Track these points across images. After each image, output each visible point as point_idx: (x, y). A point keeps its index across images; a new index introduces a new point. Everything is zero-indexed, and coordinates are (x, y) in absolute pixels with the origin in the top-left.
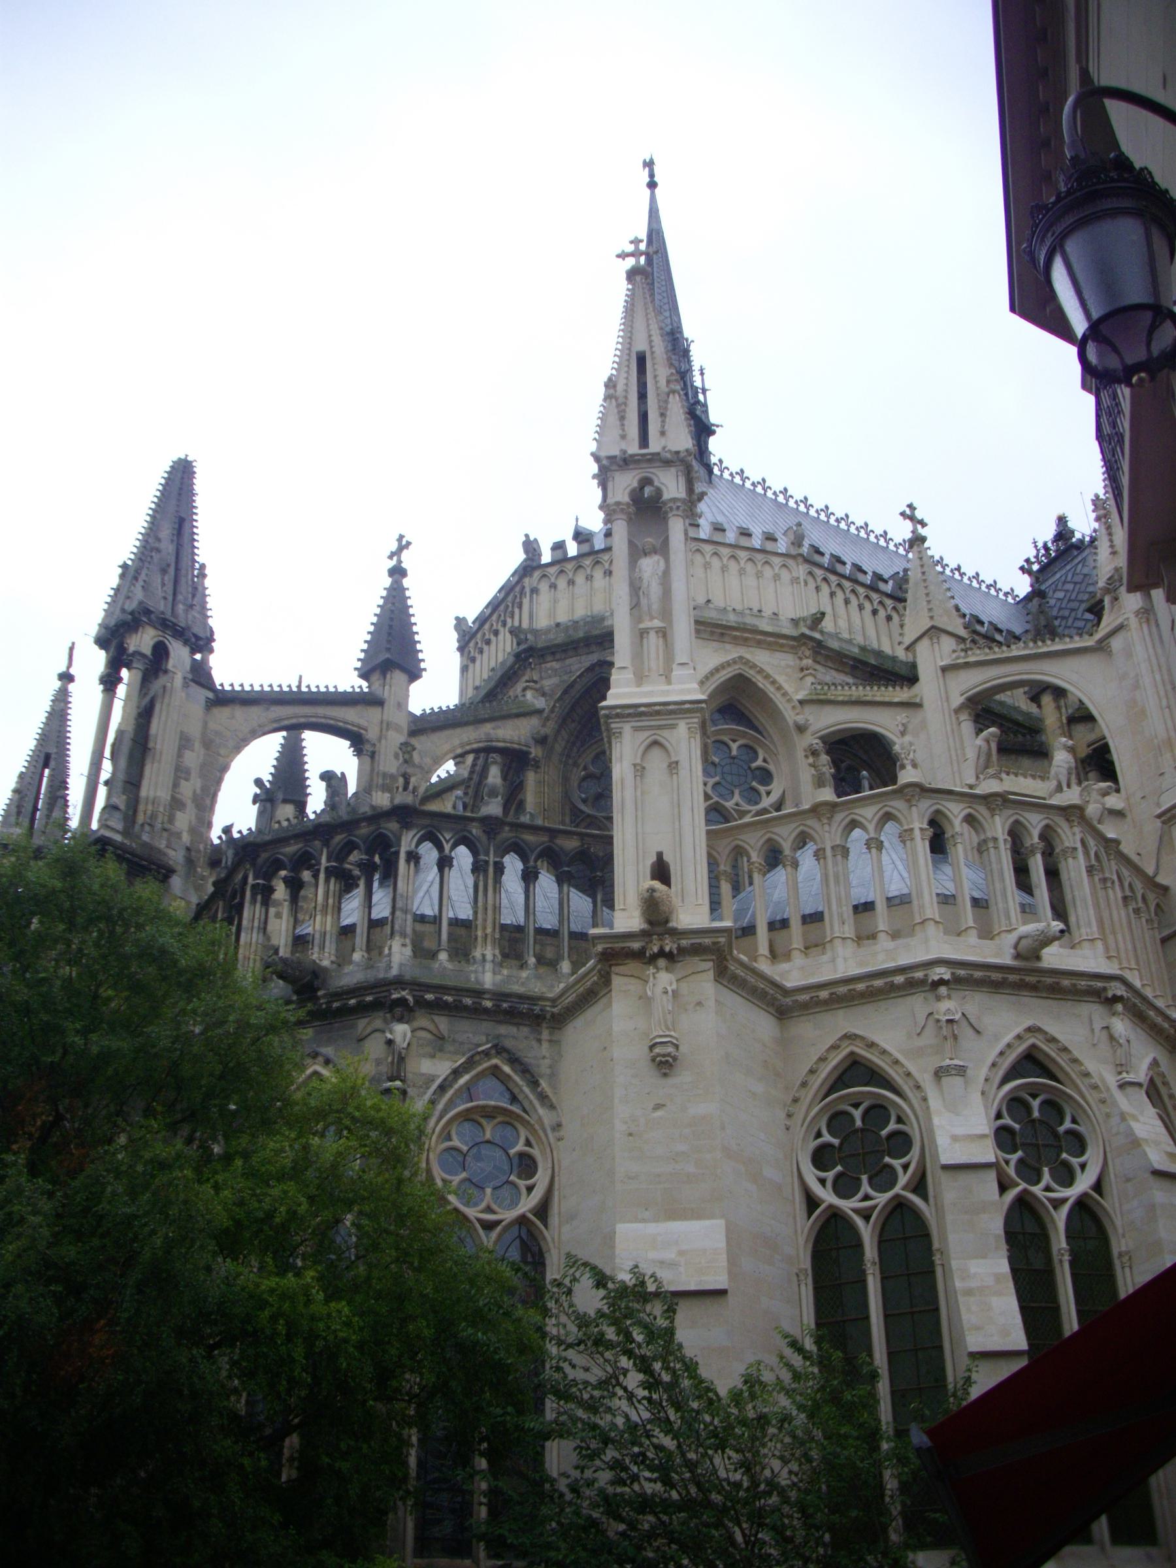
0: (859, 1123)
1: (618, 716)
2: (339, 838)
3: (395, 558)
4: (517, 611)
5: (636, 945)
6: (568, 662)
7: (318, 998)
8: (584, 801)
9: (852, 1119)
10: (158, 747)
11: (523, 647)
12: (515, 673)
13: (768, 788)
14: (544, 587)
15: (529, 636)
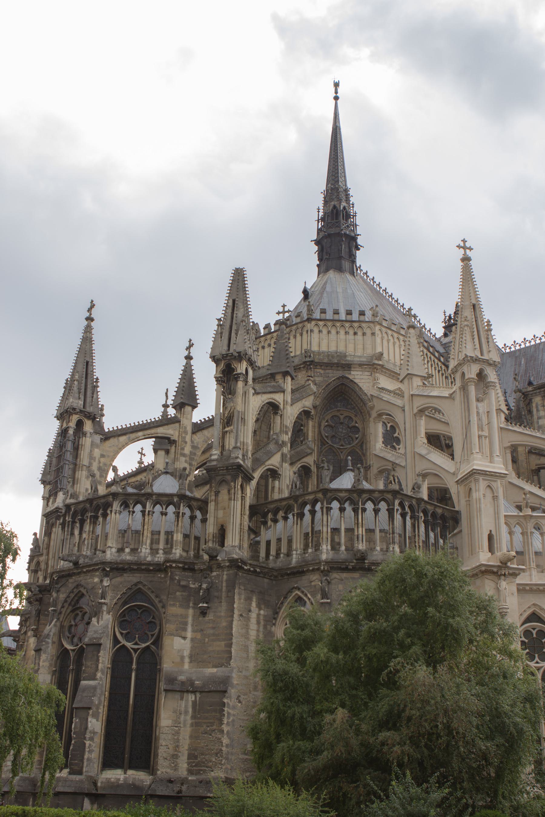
0: (535, 636)
1: (479, 473)
2: (365, 496)
3: (281, 315)
4: (298, 335)
5: (495, 570)
6: (327, 371)
7: (365, 563)
8: (326, 437)
9: (532, 634)
10: (246, 418)
11: (308, 359)
12: (300, 368)
13: (399, 447)
14: (316, 330)
15: (312, 355)
